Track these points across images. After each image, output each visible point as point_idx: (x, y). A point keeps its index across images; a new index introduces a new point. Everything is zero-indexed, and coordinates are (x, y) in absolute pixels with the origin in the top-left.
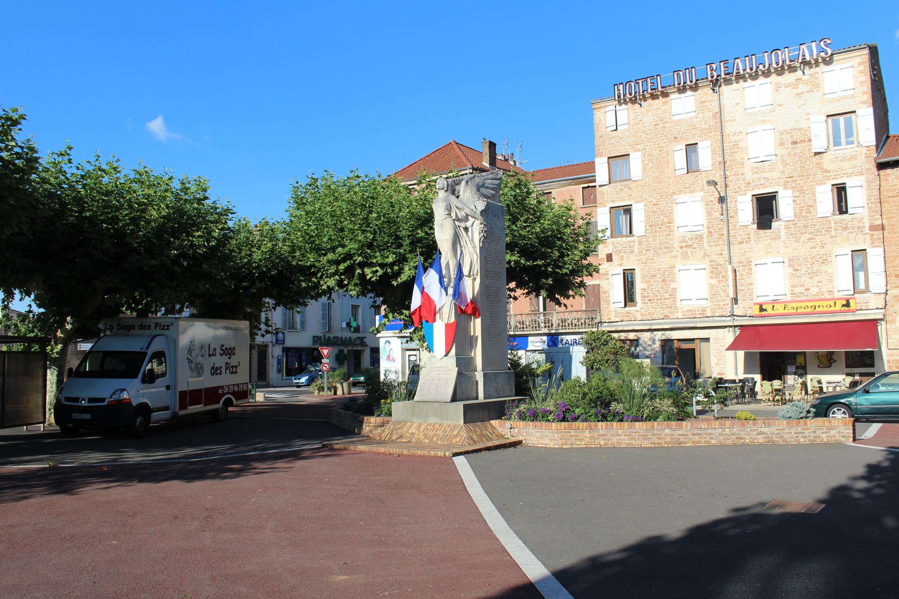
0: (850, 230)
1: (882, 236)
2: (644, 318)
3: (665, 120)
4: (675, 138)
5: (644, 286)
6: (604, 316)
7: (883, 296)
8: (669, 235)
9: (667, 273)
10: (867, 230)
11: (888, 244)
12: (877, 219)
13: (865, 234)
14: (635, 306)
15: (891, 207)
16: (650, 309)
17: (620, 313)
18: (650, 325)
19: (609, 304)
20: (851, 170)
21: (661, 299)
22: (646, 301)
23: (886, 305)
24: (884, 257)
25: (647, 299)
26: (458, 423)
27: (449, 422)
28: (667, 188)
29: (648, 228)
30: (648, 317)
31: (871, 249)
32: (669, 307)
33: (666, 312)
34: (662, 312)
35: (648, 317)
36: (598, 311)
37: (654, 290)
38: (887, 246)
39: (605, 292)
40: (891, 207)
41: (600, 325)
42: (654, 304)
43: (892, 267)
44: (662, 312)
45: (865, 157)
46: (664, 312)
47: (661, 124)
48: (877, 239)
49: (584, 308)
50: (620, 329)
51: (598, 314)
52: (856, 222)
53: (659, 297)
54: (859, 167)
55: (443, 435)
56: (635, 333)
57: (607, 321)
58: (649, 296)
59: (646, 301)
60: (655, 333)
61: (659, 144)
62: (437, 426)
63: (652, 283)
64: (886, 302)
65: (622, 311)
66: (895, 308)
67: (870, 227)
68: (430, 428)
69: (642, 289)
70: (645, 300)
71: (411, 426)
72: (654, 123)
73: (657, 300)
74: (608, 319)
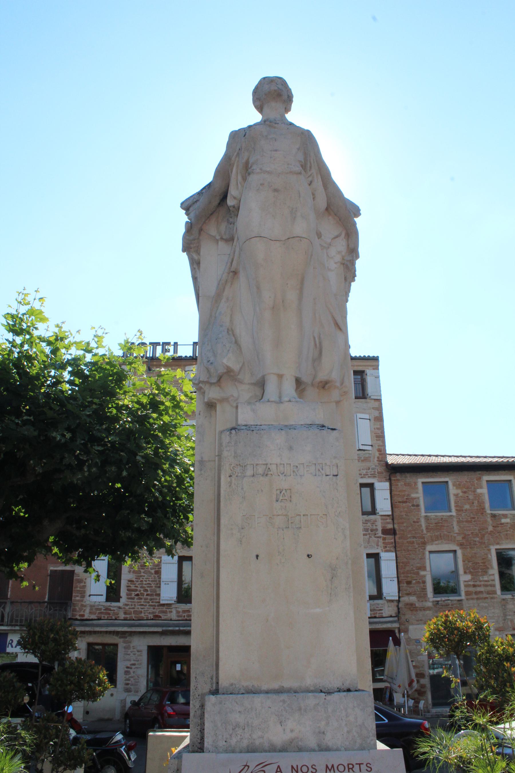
1: (393, 541)
5: (132, 577)
10: (379, 533)
11: (399, 549)
12: (388, 523)
13: (378, 537)
16: (137, 606)
19: (83, 597)
20: (364, 472)
21: (152, 595)
22: (133, 596)
23: (399, 612)
24: (397, 563)
25: (134, 593)
30: (133, 615)
33: (157, 611)
34: (151, 610)
37: (144, 582)
38: (399, 551)
39: (80, 581)
42: (143, 600)
43: (403, 573)
44: (151, 610)
45: (377, 461)
46: (154, 610)
49: (46, 600)
52: (369, 524)
53: (149, 593)
57: (79, 618)
58: (136, 590)
59: (133, 596)
63: (142, 574)
64: (398, 609)
66: (407, 617)
67: (382, 530)
69: (129, 581)
70: (131, 595)
73: (147, 595)
74: (80, 615)
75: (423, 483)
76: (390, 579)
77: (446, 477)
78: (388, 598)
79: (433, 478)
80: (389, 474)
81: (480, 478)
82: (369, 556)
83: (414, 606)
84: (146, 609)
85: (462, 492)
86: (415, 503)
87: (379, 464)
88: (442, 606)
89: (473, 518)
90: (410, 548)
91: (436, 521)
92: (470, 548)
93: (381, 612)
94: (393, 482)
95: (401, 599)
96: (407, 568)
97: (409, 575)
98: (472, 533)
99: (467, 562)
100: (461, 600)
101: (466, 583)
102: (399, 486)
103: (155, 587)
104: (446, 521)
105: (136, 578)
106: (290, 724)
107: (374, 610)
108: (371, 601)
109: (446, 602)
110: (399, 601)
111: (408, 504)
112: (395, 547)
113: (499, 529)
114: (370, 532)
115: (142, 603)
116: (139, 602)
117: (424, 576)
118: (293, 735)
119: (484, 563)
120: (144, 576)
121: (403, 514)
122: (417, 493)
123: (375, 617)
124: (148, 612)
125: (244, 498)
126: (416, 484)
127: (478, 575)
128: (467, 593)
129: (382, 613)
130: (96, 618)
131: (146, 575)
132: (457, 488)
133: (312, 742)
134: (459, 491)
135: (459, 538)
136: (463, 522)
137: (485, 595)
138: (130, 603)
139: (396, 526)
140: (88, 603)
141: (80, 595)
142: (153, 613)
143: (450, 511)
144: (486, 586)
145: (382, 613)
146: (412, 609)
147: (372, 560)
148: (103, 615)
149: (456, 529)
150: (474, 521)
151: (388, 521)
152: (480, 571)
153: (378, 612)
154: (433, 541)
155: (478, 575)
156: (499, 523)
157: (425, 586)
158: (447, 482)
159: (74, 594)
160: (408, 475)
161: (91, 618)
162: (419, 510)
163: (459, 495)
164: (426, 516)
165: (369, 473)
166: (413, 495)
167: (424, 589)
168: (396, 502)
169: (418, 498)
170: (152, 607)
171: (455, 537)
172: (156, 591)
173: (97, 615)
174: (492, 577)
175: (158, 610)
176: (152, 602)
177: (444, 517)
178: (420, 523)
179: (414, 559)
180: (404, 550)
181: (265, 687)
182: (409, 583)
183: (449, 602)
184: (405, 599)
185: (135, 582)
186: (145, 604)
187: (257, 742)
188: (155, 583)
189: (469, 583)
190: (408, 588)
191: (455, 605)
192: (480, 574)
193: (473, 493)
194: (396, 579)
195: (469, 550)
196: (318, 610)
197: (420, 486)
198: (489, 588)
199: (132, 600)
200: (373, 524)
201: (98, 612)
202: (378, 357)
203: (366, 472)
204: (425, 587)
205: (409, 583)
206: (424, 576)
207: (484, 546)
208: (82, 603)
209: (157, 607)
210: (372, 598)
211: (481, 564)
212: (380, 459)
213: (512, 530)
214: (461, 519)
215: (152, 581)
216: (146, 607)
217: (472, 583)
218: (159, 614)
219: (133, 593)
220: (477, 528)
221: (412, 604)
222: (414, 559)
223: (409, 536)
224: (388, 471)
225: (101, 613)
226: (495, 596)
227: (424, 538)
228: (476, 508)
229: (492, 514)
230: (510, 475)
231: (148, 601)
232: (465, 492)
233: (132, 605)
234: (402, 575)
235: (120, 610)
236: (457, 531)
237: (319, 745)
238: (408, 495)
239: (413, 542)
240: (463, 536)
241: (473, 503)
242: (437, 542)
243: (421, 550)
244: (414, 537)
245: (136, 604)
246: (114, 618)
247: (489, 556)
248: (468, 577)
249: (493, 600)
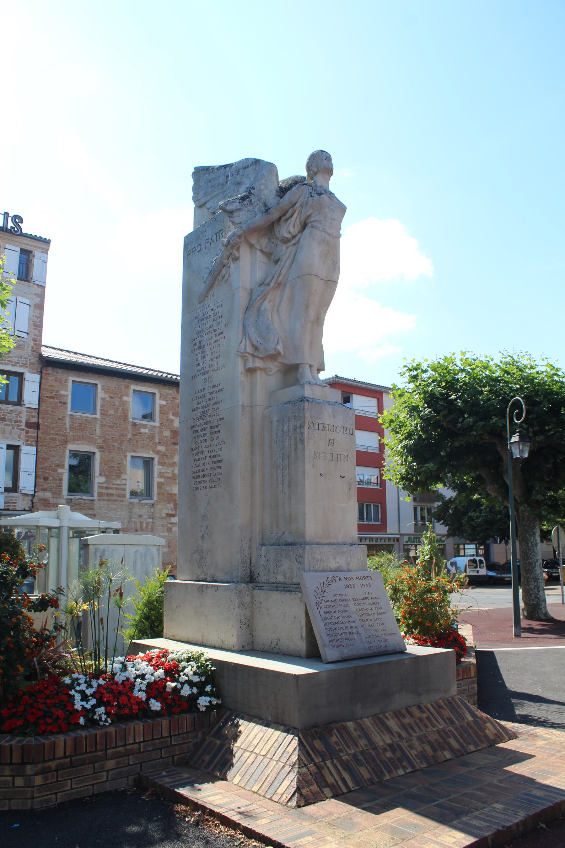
0: (7, 423)
1: (35, 435)
7: (30, 498)
10: (23, 426)
12: (33, 417)
13: (21, 429)
15: (47, 407)
20: (16, 360)
23: (33, 506)
31: (24, 446)
40: (47, 407)
43: (42, 469)
45: (31, 350)
48: (30, 437)
52: (13, 415)
54: (24, 358)
64: (33, 503)
67: (26, 423)
75: (73, 381)
76: (28, 473)
77: (96, 380)
78: (23, 492)
79: (84, 378)
80: (40, 366)
81: (128, 386)
82: (9, 447)
83: (48, 502)
85: (109, 397)
86: (63, 401)
87: (32, 354)
88: (75, 504)
89: (116, 424)
90: (51, 445)
91: (81, 422)
92: (109, 452)
93: (15, 505)
94: (44, 375)
95: (36, 494)
96: (46, 464)
97: (47, 471)
98: (112, 438)
99: (103, 465)
100: (93, 500)
101: (100, 485)
102: (50, 380)
104: (90, 422)
106: (338, 559)
107: (8, 502)
108: (6, 493)
109: (79, 500)
110: (34, 496)
111: (55, 400)
112: (37, 442)
113: (137, 437)
114: (13, 423)
117: (62, 474)
118: (339, 565)
119: (119, 467)
121: (50, 409)
122: (66, 390)
123: (8, 510)
125: (315, 441)
126: (66, 381)
127: (112, 479)
128: (100, 494)
129: (16, 506)
132: (105, 393)
133: (345, 567)
134: (107, 396)
135: (100, 441)
136: (105, 426)
137: (115, 498)
139: (40, 421)
143: (95, 413)
144: (118, 489)
145: (16, 506)
146: (46, 504)
147: (12, 452)
149: (98, 432)
150: (116, 427)
151: (33, 414)
152: (115, 474)
153: (12, 505)
154: (74, 440)
155: (112, 479)
156: (138, 432)
157: (61, 484)
158: (96, 385)
160: (60, 371)
162: (66, 408)
163: (106, 400)
164: (71, 415)
165: (20, 362)
166: (63, 393)
167: (60, 486)
168: (44, 397)
169: (67, 396)
171: (96, 440)
174: (124, 482)
177: (89, 419)
178: (64, 421)
179: (54, 456)
180: (45, 446)
181: (324, 542)
182: (46, 479)
183: (82, 500)
184: (40, 494)
187: (325, 568)
189: (103, 485)
190: (45, 484)
191: (87, 505)
192: (114, 477)
193: (119, 400)
194: (34, 474)
195: (107, 453)
196: (344, 505)
197: (70, 384)
198: (120, 492)
200: (18, 415)
202: (50, 240)
203: (18, 360)
204: (61, 485)
205: (46, 479)
206: (62, 474)
207: (121, 452)
210: (7, 490)
211: (116, 469)
212: (34, 349)
213: (148, 440)
214: (104, 423)
217: (105, 485)
220: (118, 434)
221: (46, 500)
222: (54, 456)
223: (52, 432)
224: (41, 364)
226: (124, 499)
227: (66, 436)
228: (119, 414)
229: (133, 422)
230: (155, 388)
232: (112, 398)
234: (40, 471)
236: (99, 434)
237: (348, 569)
238: (57, 391)
239: (55, 439)
240: (103, 439)
241: (118, 409)
242: (78, 442)
243: (62, 448)
244: (57, 434)
247: (125, 462)
248: (103, 479)
249: (122, 503)
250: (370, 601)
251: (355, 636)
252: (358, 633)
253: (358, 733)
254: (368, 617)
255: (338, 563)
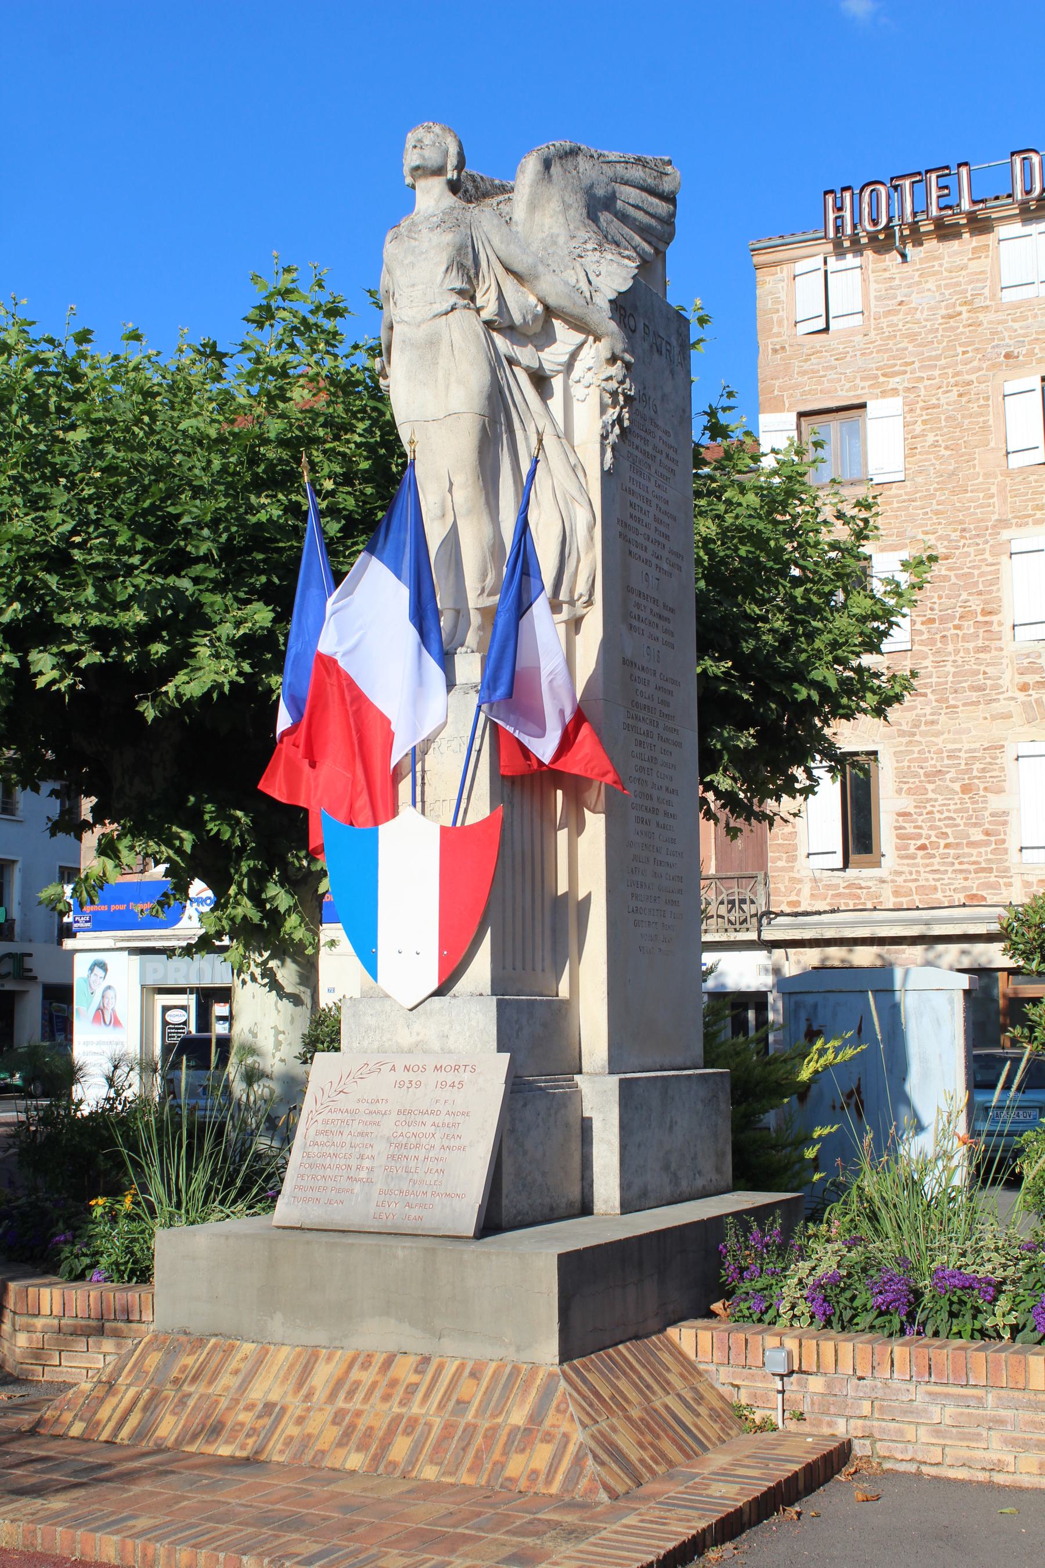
2: (905, 902)
3: (979, 302)
4: (1007, 356)
5: (906, 803)
6: (777, 890)
8: (985, 649)
9: (977, 766)
14: (878, 864)
16: (923, 875)
17: (828, 887)
18: (927, 923)
19: (793, 859)
22: (912, 850)
25: (913, 844)
26: (526, 1356)
27: (476, 1350)
28: (981, 506)
29: (918, 626)
30: (916, 898)
32: (983, 870)
33: (974, 885)
35: (916, 898)
36: (761, 877)
37: (937, 816)
41: (765, 921)
42: (937, 860)
44: (959, 883)
47: (965, 315)
50: (829, 934)
51: (760, 889)
53: (951, 840)
55: (448, 1429)
56: (875, 949)
57: (788, 910)
58: (919, 836)
59: (912, 850)
60: (940, 948)
61: (956, 374)
62: (404, 1370)
63: (931, 795)
65: (835, 881)
68: (367, 1377)
69: (899, 815)
70: (906, 847)
71: (260, 1362)
72: (943, 312)
73: (947, 846)
74: (790, 904)
84: (946, 882)
103: (965, 825)
105: (916, 807)
115: (936, 867)
116: (927, 865)
118: (420, 1038)
120: (936, 800)
124: (952, 887)
130: (828, 908)
131: (940, 797)
133: (436, 1046)
138: (906, 869)
140: (805, 873)
141: (785, 856)
142: (965, 888)
148: (842, 901)
159: (770, 854)
161: (814, 909)
170: (960, 876)
172: (968, 836)
173: (828, 900)
175: (977, 882)
176: (961, 863)
185: (915, 816)
186: (942, 868)
188: (965, 815)
199: (912, 861)
201: (831, 893)
208: (792, 874)
209: (973, 875)
215: (956, 811)
216: (945, 877)
218: (980, 893)
219: (912, 842)
225: (839, 895)
231: (950, 860)
233: (911, 873)
235: (884, 885)
237: (442, 1049)
245: (921, 869)
246: (870, 906)
250: (438, 1120)
251: (357, 1187)
252: (370, 1181)
253: (242, 1365)
254: (413, 1153)
255: (418, 1034)
